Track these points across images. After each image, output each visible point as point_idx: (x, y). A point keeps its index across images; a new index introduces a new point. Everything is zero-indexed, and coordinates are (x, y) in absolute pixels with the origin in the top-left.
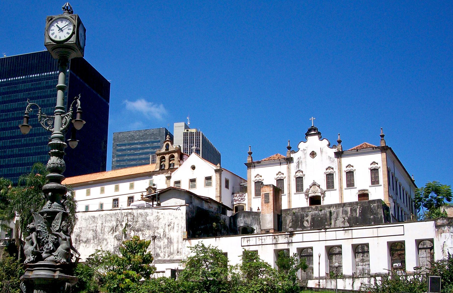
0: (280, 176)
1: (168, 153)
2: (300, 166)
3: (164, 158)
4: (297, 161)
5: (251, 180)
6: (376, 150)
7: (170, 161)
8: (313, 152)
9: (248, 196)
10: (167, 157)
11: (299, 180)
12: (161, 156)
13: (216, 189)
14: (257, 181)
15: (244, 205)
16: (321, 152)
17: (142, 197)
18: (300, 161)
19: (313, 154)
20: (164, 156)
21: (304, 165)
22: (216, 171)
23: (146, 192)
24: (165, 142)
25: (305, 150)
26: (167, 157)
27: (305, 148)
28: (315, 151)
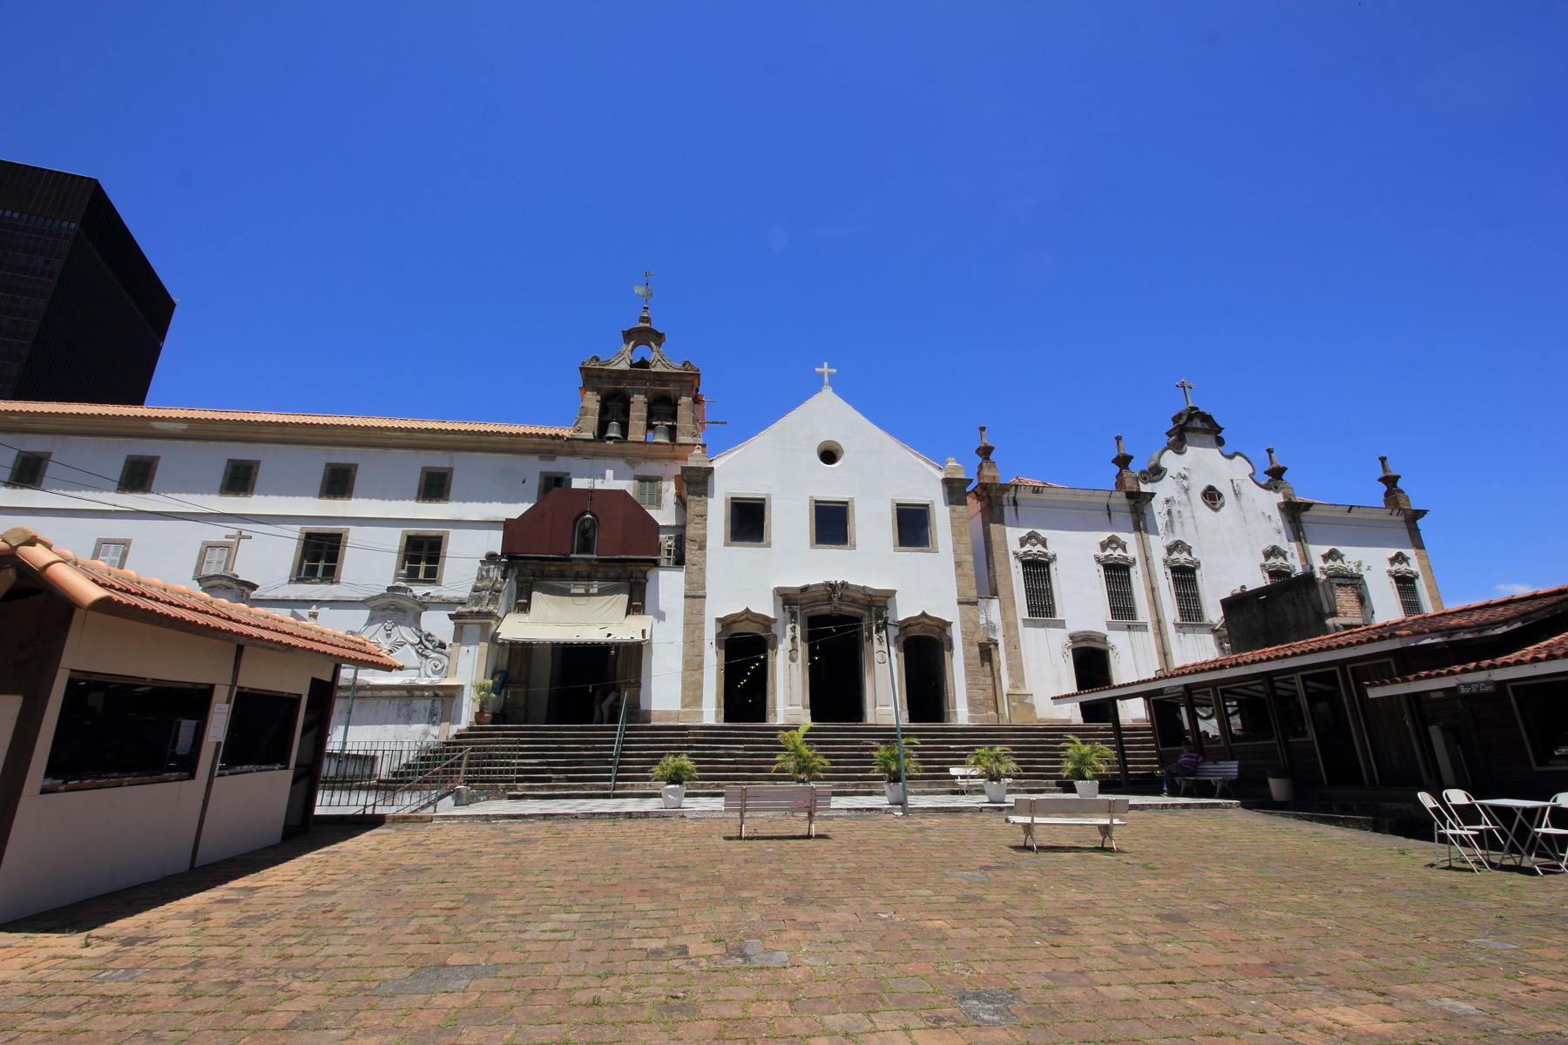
2: (1177, 526)
4: (1165, 511)
5: (1007, 551)
6: (1397, 518)
8: (1211, 488)
9: (1003, 609)
11: (1184, 576)
13: (958, 564)
15: (992, 646)
16: (1237, 494)
18: (1174, 513)
19: (1212, 496)
21: (1189, 528)
25: (1185, 478)
27: (1184, 472)
28: (1203, 487)
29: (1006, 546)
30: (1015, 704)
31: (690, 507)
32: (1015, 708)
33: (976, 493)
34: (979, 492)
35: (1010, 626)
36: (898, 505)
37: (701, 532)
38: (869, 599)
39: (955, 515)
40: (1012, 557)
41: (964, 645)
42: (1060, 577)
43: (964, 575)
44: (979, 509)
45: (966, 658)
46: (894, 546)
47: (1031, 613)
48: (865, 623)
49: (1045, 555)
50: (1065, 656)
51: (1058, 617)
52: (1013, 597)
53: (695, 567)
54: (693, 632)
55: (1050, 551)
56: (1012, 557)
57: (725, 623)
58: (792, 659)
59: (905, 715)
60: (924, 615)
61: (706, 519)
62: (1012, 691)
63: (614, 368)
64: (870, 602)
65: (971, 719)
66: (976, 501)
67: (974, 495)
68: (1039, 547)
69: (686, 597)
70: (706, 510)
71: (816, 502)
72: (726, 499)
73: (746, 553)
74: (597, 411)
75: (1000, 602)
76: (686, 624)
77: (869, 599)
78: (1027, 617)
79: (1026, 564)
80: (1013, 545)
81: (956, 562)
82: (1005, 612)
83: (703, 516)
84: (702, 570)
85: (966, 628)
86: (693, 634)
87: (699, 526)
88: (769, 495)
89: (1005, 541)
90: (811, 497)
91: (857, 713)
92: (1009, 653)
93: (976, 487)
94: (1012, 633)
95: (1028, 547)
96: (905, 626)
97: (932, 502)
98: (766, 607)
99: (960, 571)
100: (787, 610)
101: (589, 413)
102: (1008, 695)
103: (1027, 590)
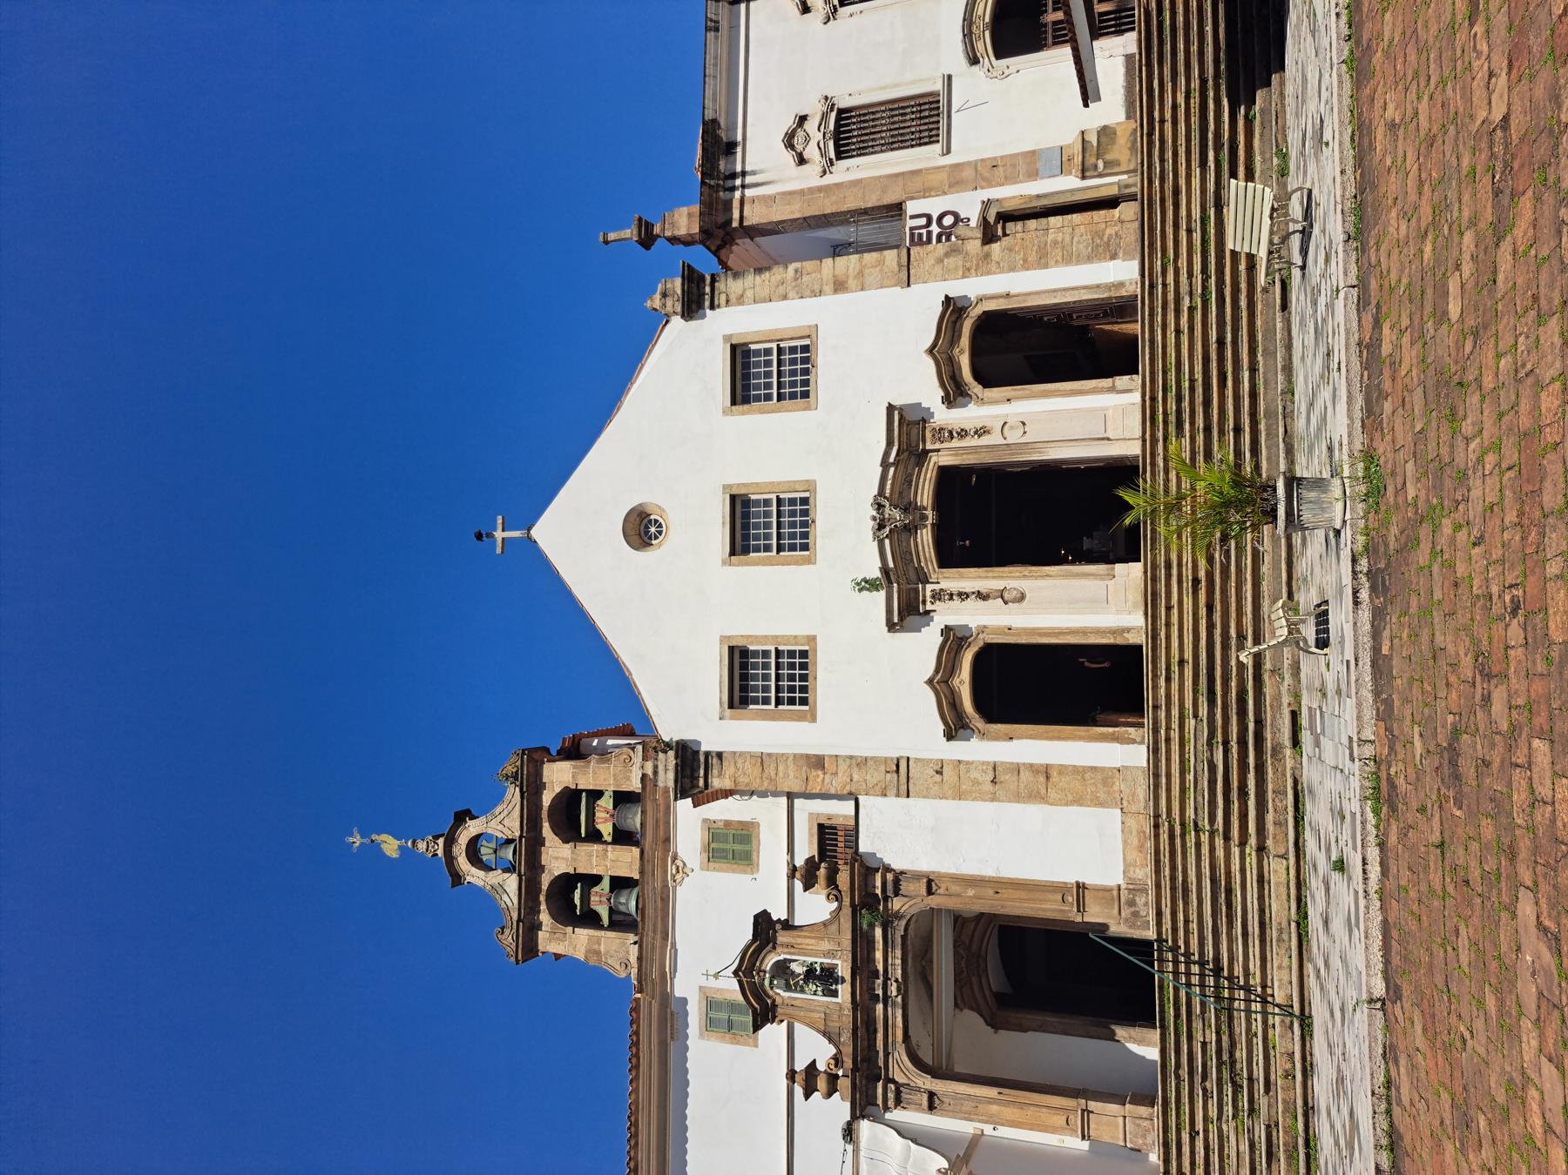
0: (817, 136)
1: (533, 842)
3: (567, 882)
5: (820, 189)
7: (595, 836)
9: (926, 193)
10: (559, 857)
12: (545, 917)
13: (840, 286)
14: (831, 144)
17: (822, 1083)
20: (552, 884)
22: (694, 303)
23: (799, 1028)
24: (457, 878)
26: (559, 857)
29: (811, 190)
30: (1101, 164)
31: (748, 784)
32: (1106, 164)
33: (719, 248)
34: (719, 242)
35: (957, 179)
36: (734, 402)
37: (791, 758)
38: (906, 454)
39: (749, 294)
40: (829, 179)
41: (989, 273)
42: (859, 91)
43: (861, 274)
44: (748, 240)
45: (1012, 269)
46: (807, 408)
47: (932, 140)
48: (946, 459)
49: (825, 116)
50: (1007, 72)
51: (938, 86)
52: (902, 174)
53: (856, 777)
54: (976, 782)
55: (815, 109)
56: (829, 179)
57: (956, 728)
58: (1021, 598)
59: (1122, 381)
60: (931, 351)
61: (770, 755)
62: (1077, 170)
63: (516, 901)
64: (911, 453)
65: (1128, 256)
66: (734, 248)
67: (723, 253)
68: (811, 126)
69: (908, 796)
70: (752, 755)
71: (733, 553)
72: (732, 718)
73: (826, 680)
74: (592, 932)
75: (912, 198)
76: (960, 796)
77: (906, 454)
78: (936, 148)
79: (840, 155)
80: (810, 177)
81: (836, 291)
82: (931, 189)
83: (762, 759)
84: (862, 762)
85: (956, 269)
86: (979, 783)
87: (781, 768)
88: (723, 639)
89: (802, 192)
90: (724, 563)
91: (1123, 472)
92: (1006, 178)
93: (708, 248)
94: (968, 173)
95: (812, 152)
96: (955, 393)
97: (727, 338)
98: (924, 645)
99: (852, 283)
100: (929, 607)
101: (596, 947)
102: (1083, 178)
103: (891, 146)
